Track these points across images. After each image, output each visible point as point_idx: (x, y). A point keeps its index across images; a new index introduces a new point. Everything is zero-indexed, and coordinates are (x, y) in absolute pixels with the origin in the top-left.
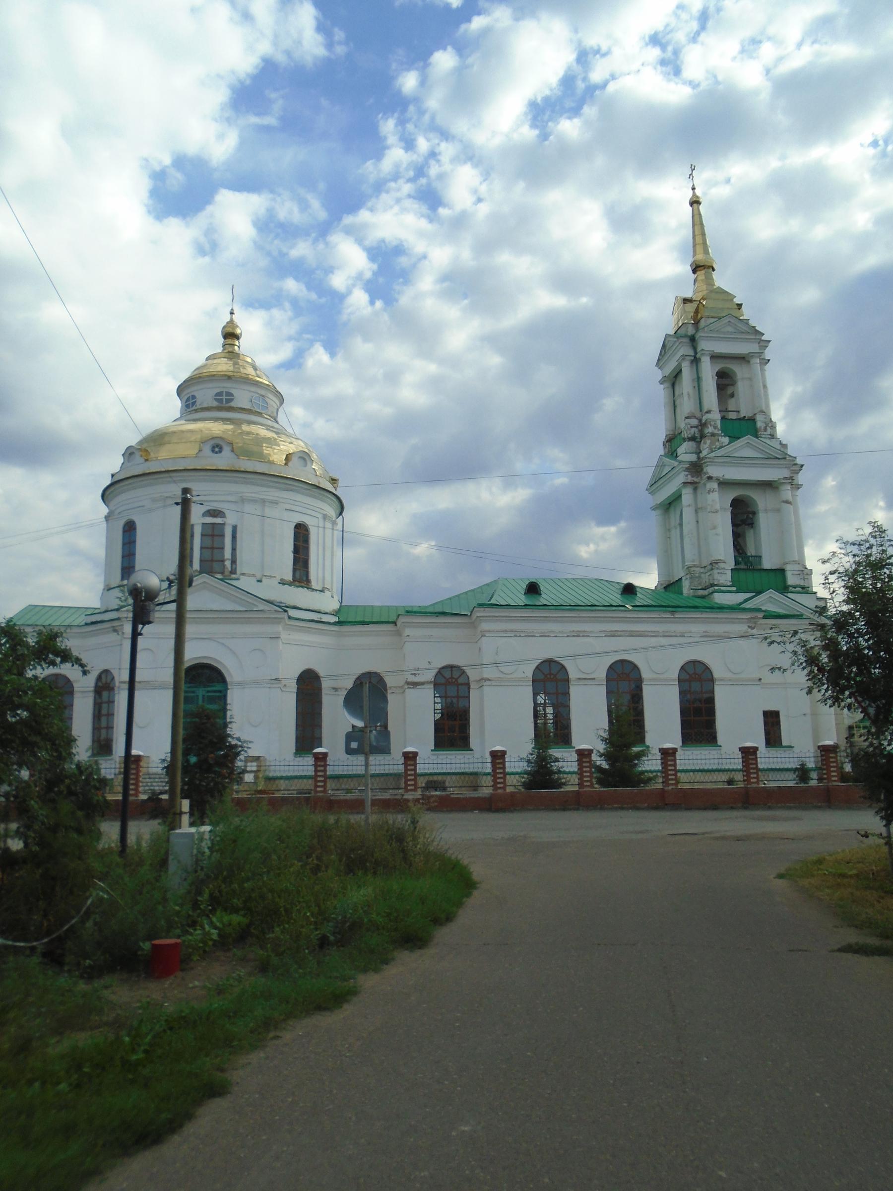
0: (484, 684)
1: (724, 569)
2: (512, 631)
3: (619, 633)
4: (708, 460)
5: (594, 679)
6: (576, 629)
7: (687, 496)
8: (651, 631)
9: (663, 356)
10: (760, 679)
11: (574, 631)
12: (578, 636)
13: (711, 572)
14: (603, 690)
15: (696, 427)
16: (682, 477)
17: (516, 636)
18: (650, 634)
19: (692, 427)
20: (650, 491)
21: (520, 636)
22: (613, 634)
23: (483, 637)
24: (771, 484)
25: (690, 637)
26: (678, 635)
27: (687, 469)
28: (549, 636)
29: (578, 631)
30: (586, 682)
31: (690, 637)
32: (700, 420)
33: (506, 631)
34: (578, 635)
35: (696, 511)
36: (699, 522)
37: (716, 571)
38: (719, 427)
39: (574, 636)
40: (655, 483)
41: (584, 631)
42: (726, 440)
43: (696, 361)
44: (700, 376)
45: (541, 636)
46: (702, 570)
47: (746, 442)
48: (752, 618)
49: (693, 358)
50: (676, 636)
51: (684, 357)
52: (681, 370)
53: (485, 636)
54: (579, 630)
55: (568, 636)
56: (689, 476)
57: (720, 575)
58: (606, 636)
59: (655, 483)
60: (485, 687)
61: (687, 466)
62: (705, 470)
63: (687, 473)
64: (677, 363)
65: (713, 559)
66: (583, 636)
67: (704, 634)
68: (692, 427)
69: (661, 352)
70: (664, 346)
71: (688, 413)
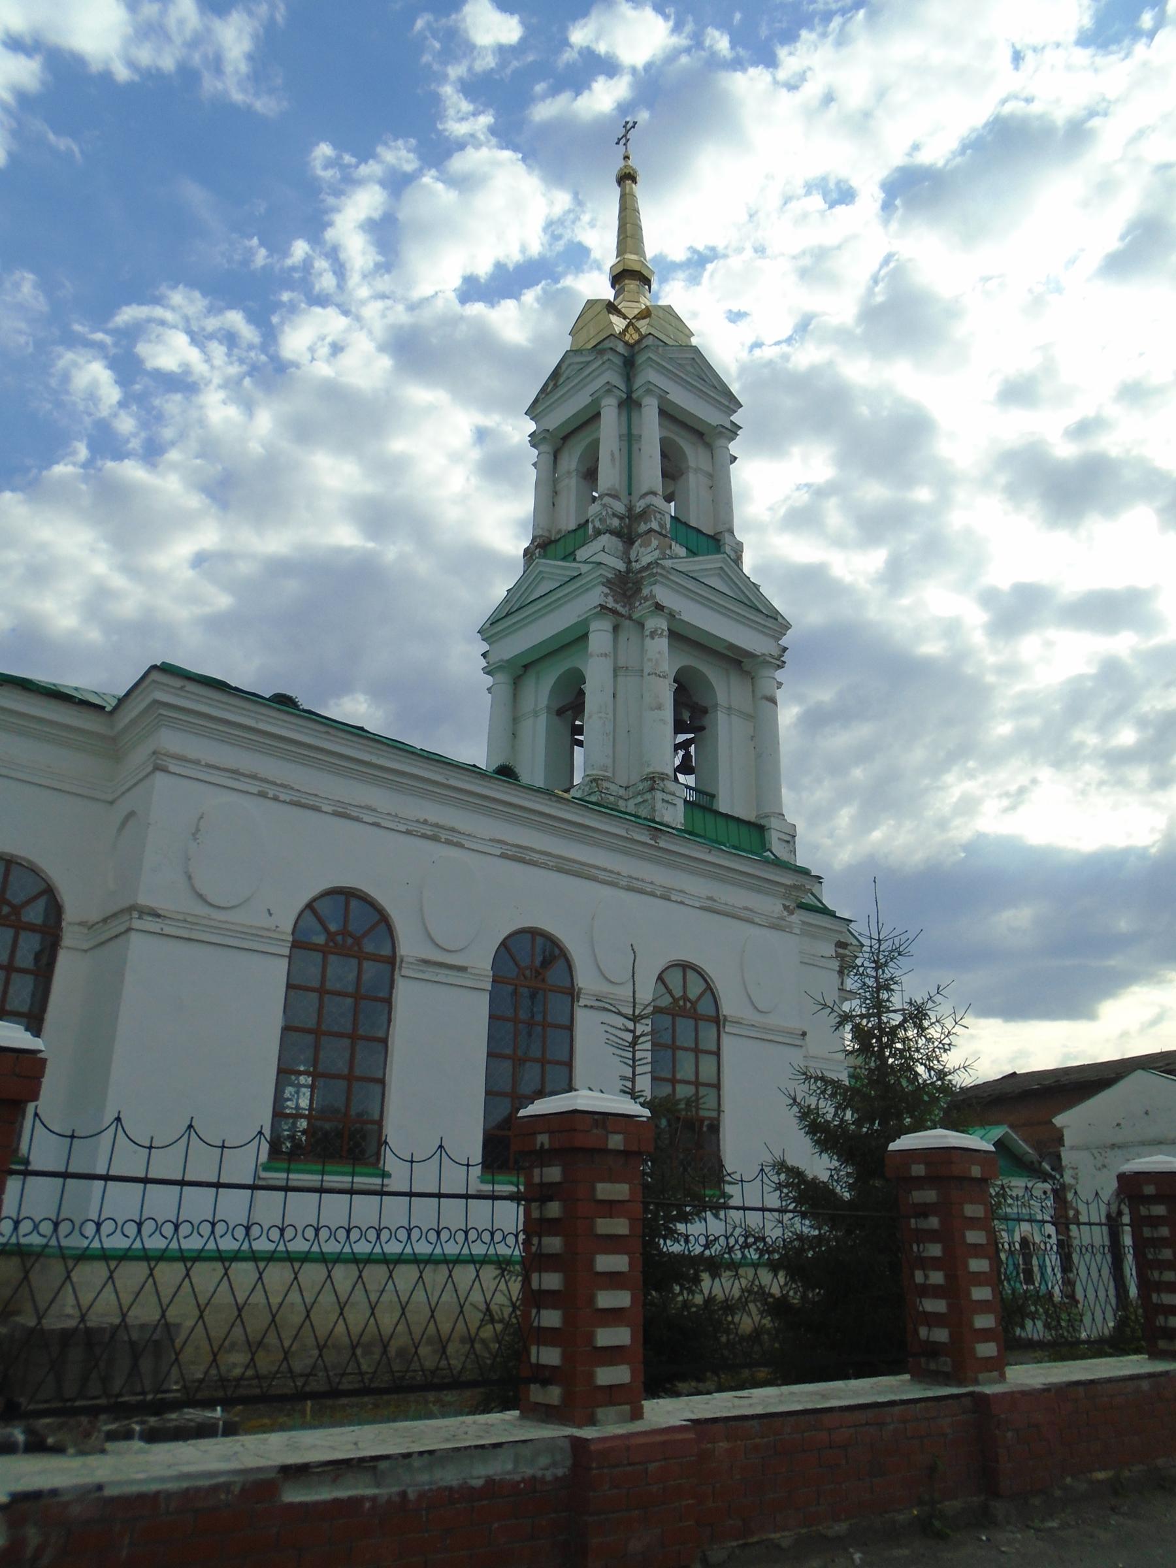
0: (137, 924)
1: (674, 794)
2: (254, 777)
3: (536, 857)
4: (660, 571)
5: (462, 969)
6: (432, 819)
7: (600, 637)
8: (605, 870)
9: (547, 394)
10: (804, 1034)
11: (425, 822)
12: (434, 838)
13: (648, 796)
14: (481, 1005)
15: (621, 518)
16: (597, 596)
17: (262, 795)
18: (602, 875)
19: (614, 515)
20: (485, 636)
21: (276, 799)
22: (519, 856)
23: (159, 775)
24: (747, 664)
25: (682, 903)
26: (659, 893)
27: (608, 583)
28: (357, 819)
29: (437, 825)
30: (443, 975)
31: (682, 903)
32: (630, 509)
33: (235, 773)
34: (435, 834)
35: (616, 671)
36: (618, 696)
37: (659, 795)
38: (668, 526)
39: (424, 836)
40: (507, 615)
41: (453, 830)
42: (682, 552)
43: (629, 404)
44: (635, 431)
45: (336, 814)
46: (622, 792)
47: (719, 565)
48: (795, 887)
49: (625, 396)
50: (653, 894)
51: (609, 389)
52: (598, 415)
53: (165, 770)
54: (441, 822)
55: (408, 833)
56: (610, 599)
57: (665, 805)
58: (503, 856)
59: (507, 615)
60: (134, 936)
61: (610, 576)
62: (645, 592)
63: (607, 590)
64: (590, 399)
65: (651, 769)
66: (448, 842)
67: (709, 903)
68: (614, 515)
69: (546, 384)
70: (556, 374)
71: (608, 489)
